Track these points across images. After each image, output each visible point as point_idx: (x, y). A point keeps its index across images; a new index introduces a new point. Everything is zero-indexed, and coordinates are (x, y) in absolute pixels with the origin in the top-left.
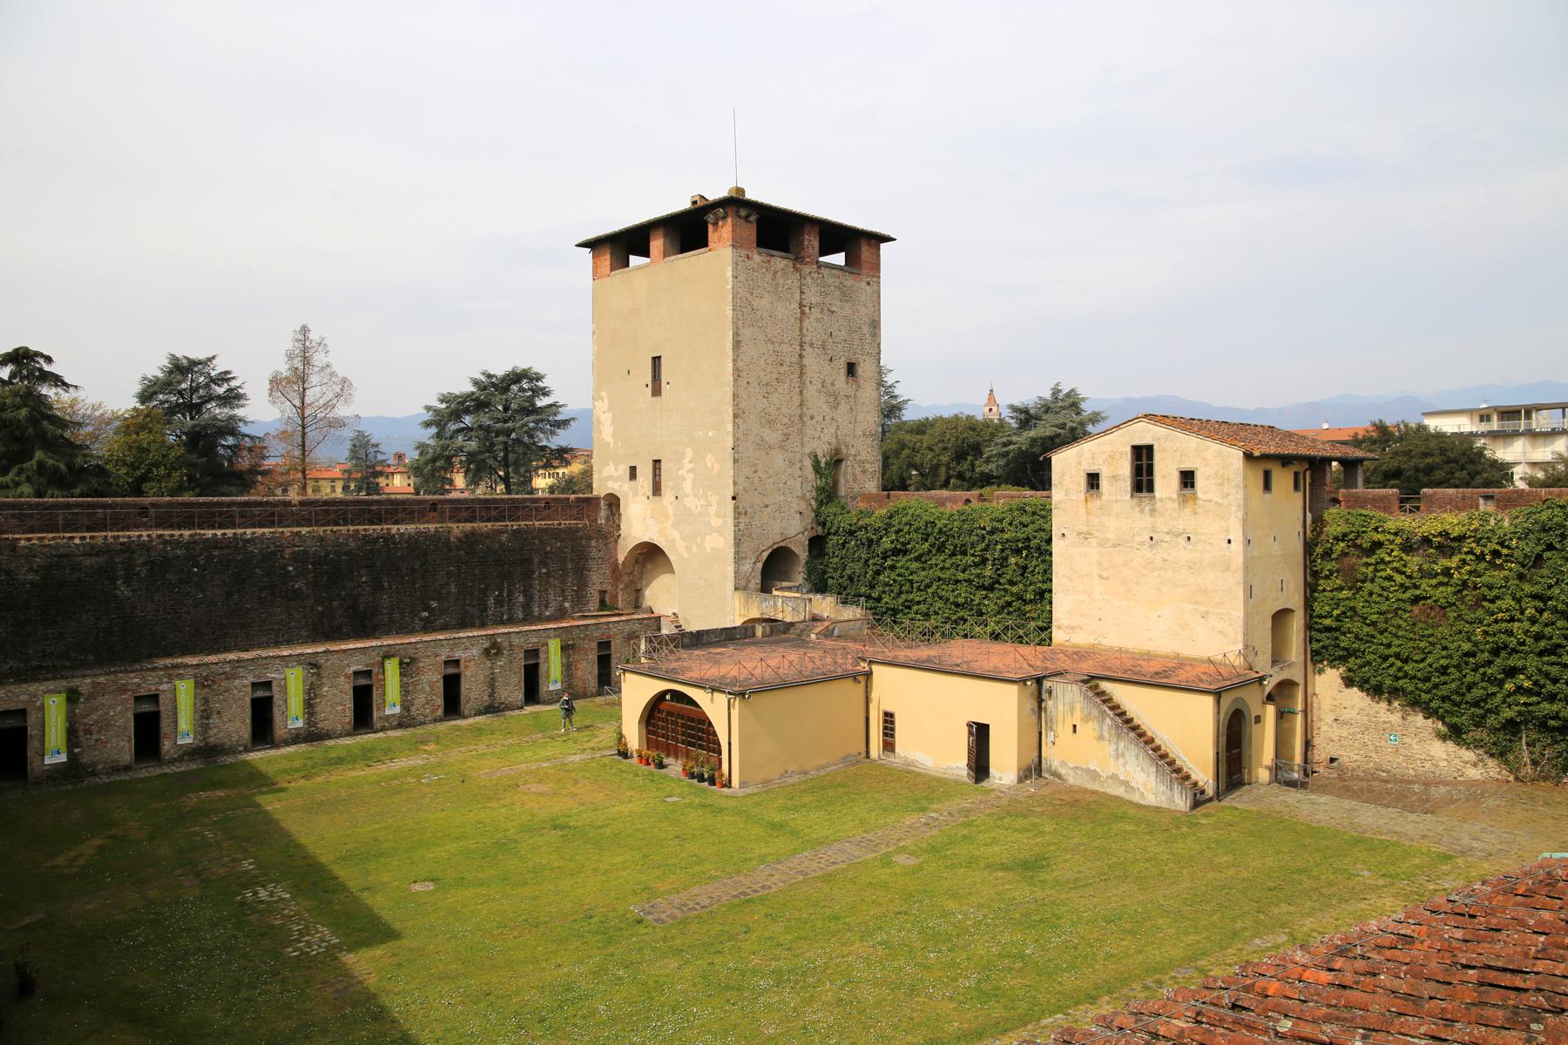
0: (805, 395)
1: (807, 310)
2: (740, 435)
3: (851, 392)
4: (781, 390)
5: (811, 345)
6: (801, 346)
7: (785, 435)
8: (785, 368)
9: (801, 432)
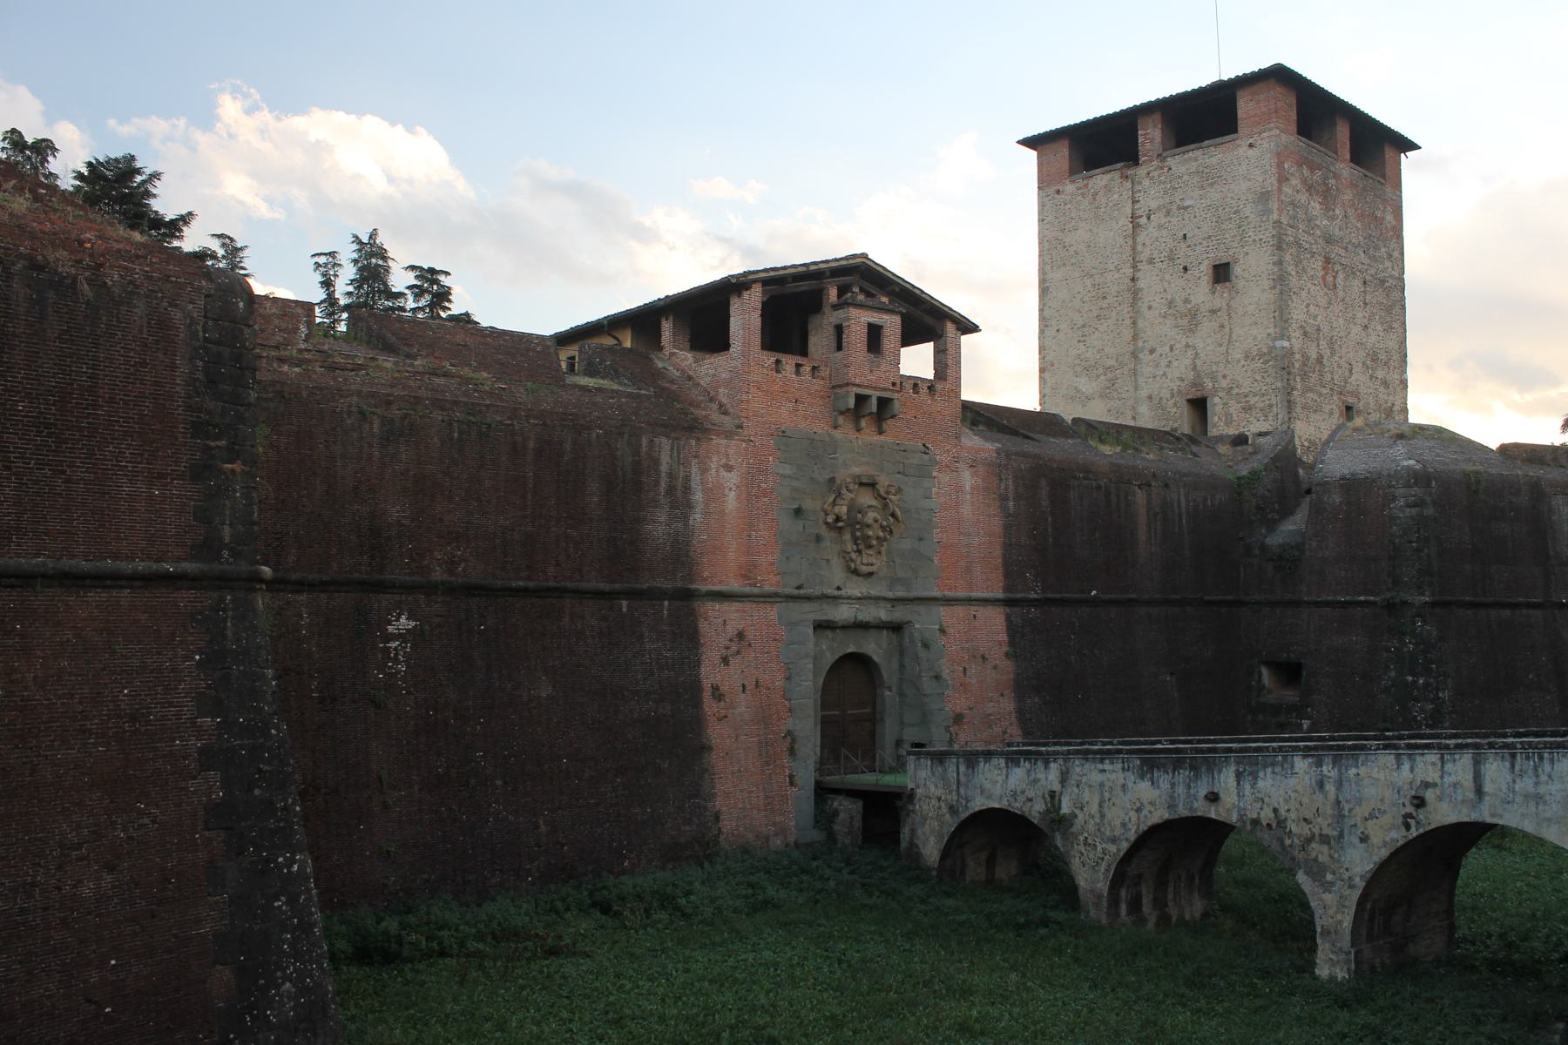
0: (1140, 324)
1: (1143, 221)
2: (1048, 390)
3: (1218, 302)
4: (1101, 328)
5: (1151, 261)
6: (1134, 267)
7: (1109, 381)
8: (1110, 300)
9: (1135, 373)
